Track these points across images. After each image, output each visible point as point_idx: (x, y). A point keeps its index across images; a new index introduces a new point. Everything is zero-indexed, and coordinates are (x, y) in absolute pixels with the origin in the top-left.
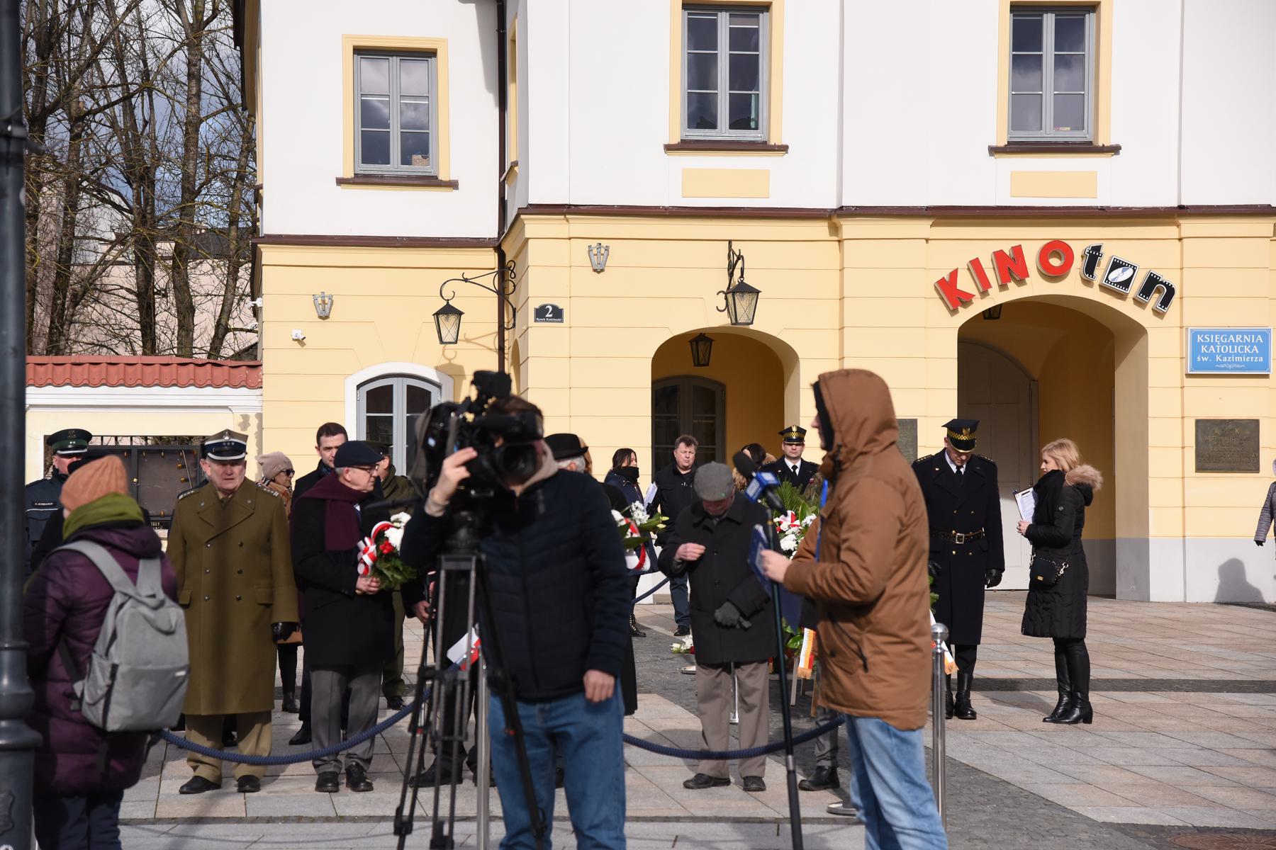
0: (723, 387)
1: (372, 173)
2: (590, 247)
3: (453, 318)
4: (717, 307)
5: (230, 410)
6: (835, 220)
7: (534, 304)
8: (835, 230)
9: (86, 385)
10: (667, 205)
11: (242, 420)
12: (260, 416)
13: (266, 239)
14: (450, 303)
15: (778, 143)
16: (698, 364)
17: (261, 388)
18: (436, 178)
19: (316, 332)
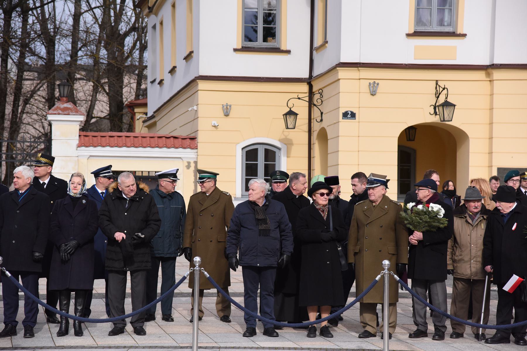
0: (415, 151)
1: (249, 46)
2: (370, 83)
3: (292, 117)
4: (430, 113)
5: (182, 159)
6: (490, 70)
7: (342, 110)
8: (488, 75)
9: (116, 146)
10: (407, 63)
11: (187, 164)
12: (196, 163)
13: (200, 78)
14: (292, 109)
15: (462, 33)
16: (410, 140)
17: (197, 149)
18: (279, 49)
19: (224, 123)
